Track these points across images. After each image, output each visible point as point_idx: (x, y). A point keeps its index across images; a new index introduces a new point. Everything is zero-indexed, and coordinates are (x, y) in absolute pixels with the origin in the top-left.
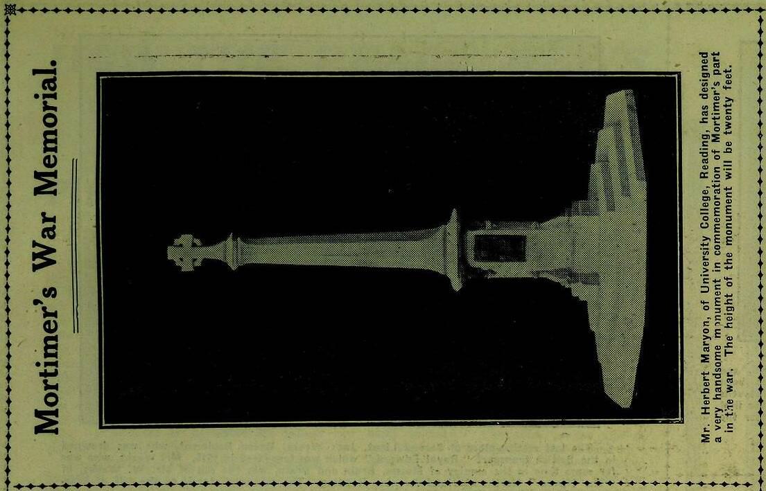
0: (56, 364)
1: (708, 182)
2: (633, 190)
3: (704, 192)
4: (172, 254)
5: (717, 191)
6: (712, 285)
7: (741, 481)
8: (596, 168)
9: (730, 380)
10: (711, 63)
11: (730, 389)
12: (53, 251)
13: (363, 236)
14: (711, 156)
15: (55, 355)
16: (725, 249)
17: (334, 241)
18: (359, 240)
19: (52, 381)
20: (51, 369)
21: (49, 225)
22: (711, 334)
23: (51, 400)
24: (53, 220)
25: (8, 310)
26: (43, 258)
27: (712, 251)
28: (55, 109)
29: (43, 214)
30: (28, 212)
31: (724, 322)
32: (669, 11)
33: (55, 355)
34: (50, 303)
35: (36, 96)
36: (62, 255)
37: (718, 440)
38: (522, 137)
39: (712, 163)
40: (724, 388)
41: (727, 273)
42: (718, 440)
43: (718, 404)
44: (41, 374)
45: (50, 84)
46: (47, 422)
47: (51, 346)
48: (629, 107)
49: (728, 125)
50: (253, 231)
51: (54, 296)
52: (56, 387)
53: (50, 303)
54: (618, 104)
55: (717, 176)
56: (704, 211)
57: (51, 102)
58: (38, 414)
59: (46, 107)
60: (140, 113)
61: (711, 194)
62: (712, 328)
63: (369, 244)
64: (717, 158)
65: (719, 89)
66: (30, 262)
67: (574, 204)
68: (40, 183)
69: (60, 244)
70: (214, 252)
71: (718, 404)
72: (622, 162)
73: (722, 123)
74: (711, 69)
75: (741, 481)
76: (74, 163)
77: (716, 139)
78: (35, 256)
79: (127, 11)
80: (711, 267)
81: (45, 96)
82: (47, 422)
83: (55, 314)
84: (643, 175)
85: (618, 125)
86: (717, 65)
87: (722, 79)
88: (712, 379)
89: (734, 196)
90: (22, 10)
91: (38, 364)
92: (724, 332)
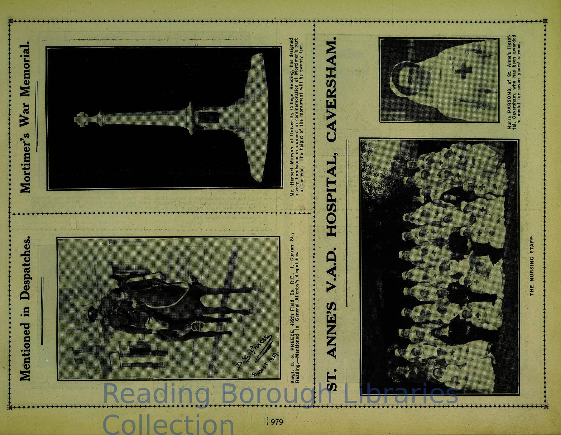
0: (29, 164)
1: (293, 91)
2: (262, 95)
3: (291, 95)
4: (76, 120)
5: (297, 95)
6: (294, 133)
7: (306, 212)
8: (247, 85)
9: (302, 171)
10: (294, 43)
11: (302, 175)
12: (28, 119)
13: (153, 113)
14: (294, 80)
15: (29, 161)
16: (300, 118)
17: (142, 115)
18: (151, 114)
19: (27, 171)
20: (27, 167)
21: (26, 108)
22: (294, 152)
23: (27, 179)
24: (28, 106)
25: (10, 143)
26: (24, 122)
27: (295, 119)
28: (29, 61)
29: (24, 104)
30: (18, 102)
31: (299, 147)
32: (277, 22)
33: (29, 161)
34: (27, 140)
35: (21, 56)
36: (32, 120)
37: (297, 195)
38: (217, 73)
39: (295, 83)
40: (299, 174)
41: (301, 128)
42: (297, 195)
43: (297, 181)
44: (23, 169)
45: (27, 51)
46: (25, 188)
47: (27, 157)
48: (261, 61)
49: (301, 68)
50: (108, 111)
51: (28, 137)
52: (29, 174)
53: (27, 140)
54: (256, 59)
55: (297, 89)
56: (291, 103)
57: (27, 58)
58: (22, 185)
59: (25, 61)
60: (62, 61)
61: (294, 96)
62: (295, 150)
63: (156, 116)
64: (297, 81)
65: (297, 53)
66: (18, 123)
67: (239, 100)
68: (23, 188)
69: (31, 116)
70: (93, 119)
71: (297, 181)
72: (258, 83)
73: (299, 67)
74: (294, 45)
75: (306, 212)
76: (37, 83)
77: (296, 73)
78: (21, 121)
79: (58, 22)
80: (294, 125)
81: (25, 56)
82: (25, 188)
83: (29, 144)
84: (267, 88)
85: (256, 68)
86: (297, 43)
87: (299, 49)
88: (295, 171)
89: (304, 96)
90: (15, 21)
91: (22, 165)
92: (299, 152)
